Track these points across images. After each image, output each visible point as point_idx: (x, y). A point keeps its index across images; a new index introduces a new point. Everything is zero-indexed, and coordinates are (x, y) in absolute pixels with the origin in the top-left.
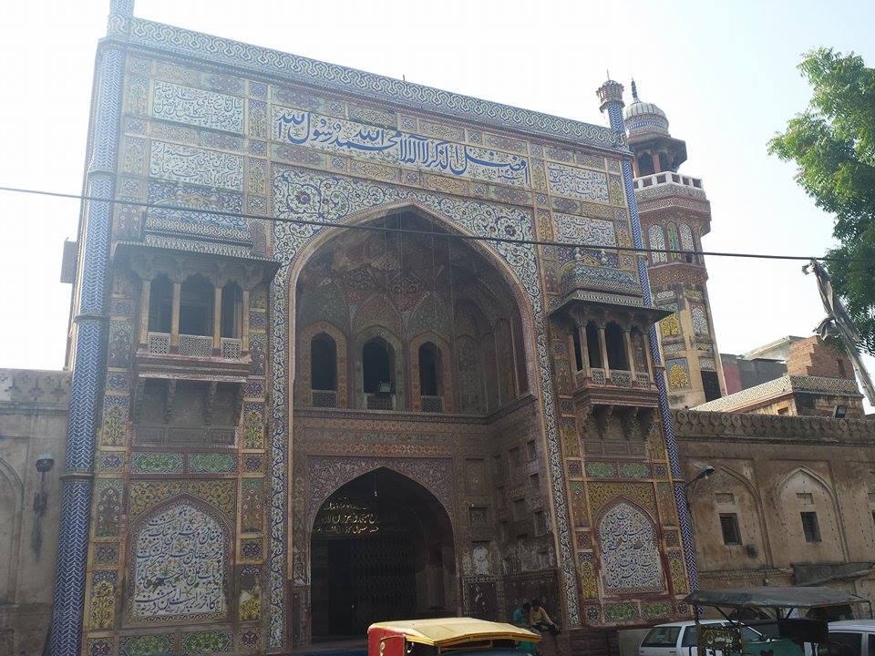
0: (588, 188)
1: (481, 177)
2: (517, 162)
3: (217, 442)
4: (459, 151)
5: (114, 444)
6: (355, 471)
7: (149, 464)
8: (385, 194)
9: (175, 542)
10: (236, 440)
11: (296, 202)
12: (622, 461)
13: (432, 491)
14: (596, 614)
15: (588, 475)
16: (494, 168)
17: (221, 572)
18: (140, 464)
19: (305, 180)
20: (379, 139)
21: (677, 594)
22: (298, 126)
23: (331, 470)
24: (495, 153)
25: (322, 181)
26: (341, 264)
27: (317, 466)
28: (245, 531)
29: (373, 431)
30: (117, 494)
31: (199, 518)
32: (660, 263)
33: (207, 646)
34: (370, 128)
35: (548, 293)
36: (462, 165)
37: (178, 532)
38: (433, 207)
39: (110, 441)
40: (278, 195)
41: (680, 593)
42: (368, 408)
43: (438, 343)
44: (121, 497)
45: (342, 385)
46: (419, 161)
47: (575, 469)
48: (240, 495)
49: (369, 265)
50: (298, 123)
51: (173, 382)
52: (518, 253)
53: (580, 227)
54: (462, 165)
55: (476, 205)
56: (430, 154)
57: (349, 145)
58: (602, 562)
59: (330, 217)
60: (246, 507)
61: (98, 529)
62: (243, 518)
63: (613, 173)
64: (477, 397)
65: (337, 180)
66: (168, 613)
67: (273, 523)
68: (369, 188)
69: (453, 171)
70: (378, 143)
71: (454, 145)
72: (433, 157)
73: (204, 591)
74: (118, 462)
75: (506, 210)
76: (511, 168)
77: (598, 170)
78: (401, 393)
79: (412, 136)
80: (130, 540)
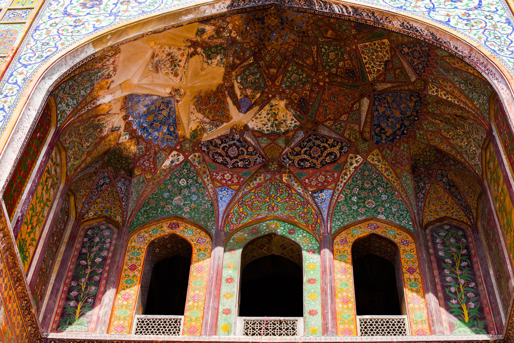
26: (193, 126)
43: (391, 234)
49: (246, 127)
52: (472, 17)
59: (127, 14)
64: (481, 310)
78: (312, 313)
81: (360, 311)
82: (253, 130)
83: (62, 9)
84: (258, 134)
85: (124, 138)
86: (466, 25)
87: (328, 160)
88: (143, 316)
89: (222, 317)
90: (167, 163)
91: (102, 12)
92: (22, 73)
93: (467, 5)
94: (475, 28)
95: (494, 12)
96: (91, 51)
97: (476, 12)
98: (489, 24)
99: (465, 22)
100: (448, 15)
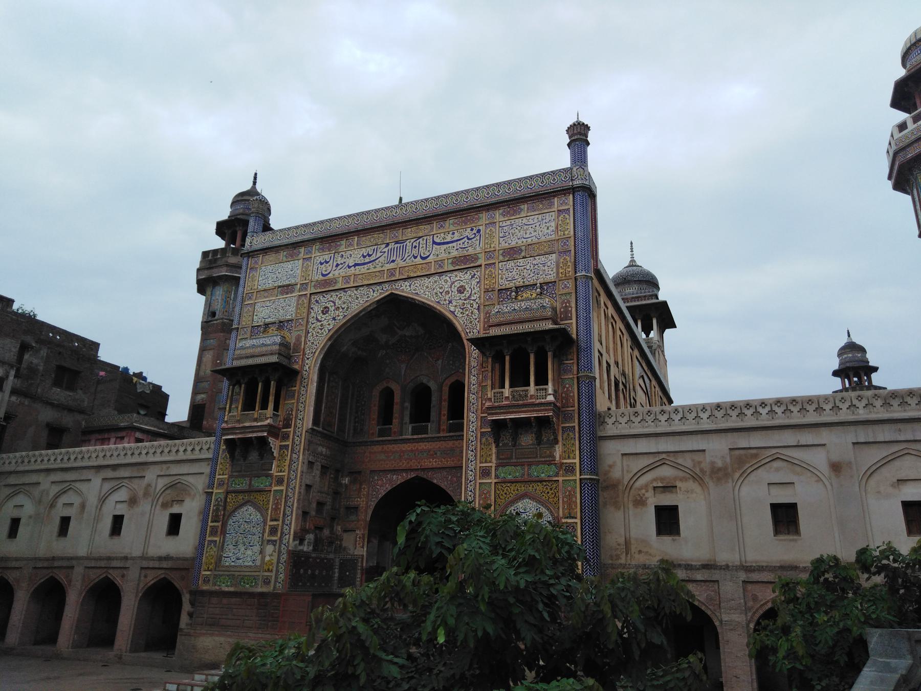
1: (443, 256)
2: (475, 231)
3: (264, 470)
4: (428, 241)
5: (223, 475)
6: (398, 479)
7: (235, 484)
8: (374, 291)
10: (273, 467)
12: (530, 464)
13: (449, 492)
15: (497, 477)
16: (454, 244)
18: (232, 484)
22: (327, 265)
23: (384, 479)
27: (376, 478)
28: (272, 520)
29: (412, 451)
30: (221, 500)
33: (248, 584)
34: (368, 249)
35: (485, 332)
38: (405, 289)
39: (221, 473)
45: (395, 421)
47: (485, 473)
48: (271, 500)
49: (405, 335)
50: (327, 262)
51: (237, 440)
54: (429, 251)
55: (436, 278)
56: (407, 251)
57: (356, 265)
59: (339, 318)
60: (274, 507)
61: (212, 518)
62: (271, 512)
63: (560, 208)
65: (346, 292)
69: (423, 258)
70: (372, 258)
71: (425, 238)
75: (460, 274)
76: (469, 239)
77: (546, 211)
78: (433, 422)
79: (397, 243)
80: (224, 525)
81: (449, 419)
86: (461, 313)
87: (439, 345)
92: (307, 364)
93: (465, 296)
94: (464, 315)
95: (474, 300)
96: (329, 343)
99: (462, 311)
100: (456, 306)
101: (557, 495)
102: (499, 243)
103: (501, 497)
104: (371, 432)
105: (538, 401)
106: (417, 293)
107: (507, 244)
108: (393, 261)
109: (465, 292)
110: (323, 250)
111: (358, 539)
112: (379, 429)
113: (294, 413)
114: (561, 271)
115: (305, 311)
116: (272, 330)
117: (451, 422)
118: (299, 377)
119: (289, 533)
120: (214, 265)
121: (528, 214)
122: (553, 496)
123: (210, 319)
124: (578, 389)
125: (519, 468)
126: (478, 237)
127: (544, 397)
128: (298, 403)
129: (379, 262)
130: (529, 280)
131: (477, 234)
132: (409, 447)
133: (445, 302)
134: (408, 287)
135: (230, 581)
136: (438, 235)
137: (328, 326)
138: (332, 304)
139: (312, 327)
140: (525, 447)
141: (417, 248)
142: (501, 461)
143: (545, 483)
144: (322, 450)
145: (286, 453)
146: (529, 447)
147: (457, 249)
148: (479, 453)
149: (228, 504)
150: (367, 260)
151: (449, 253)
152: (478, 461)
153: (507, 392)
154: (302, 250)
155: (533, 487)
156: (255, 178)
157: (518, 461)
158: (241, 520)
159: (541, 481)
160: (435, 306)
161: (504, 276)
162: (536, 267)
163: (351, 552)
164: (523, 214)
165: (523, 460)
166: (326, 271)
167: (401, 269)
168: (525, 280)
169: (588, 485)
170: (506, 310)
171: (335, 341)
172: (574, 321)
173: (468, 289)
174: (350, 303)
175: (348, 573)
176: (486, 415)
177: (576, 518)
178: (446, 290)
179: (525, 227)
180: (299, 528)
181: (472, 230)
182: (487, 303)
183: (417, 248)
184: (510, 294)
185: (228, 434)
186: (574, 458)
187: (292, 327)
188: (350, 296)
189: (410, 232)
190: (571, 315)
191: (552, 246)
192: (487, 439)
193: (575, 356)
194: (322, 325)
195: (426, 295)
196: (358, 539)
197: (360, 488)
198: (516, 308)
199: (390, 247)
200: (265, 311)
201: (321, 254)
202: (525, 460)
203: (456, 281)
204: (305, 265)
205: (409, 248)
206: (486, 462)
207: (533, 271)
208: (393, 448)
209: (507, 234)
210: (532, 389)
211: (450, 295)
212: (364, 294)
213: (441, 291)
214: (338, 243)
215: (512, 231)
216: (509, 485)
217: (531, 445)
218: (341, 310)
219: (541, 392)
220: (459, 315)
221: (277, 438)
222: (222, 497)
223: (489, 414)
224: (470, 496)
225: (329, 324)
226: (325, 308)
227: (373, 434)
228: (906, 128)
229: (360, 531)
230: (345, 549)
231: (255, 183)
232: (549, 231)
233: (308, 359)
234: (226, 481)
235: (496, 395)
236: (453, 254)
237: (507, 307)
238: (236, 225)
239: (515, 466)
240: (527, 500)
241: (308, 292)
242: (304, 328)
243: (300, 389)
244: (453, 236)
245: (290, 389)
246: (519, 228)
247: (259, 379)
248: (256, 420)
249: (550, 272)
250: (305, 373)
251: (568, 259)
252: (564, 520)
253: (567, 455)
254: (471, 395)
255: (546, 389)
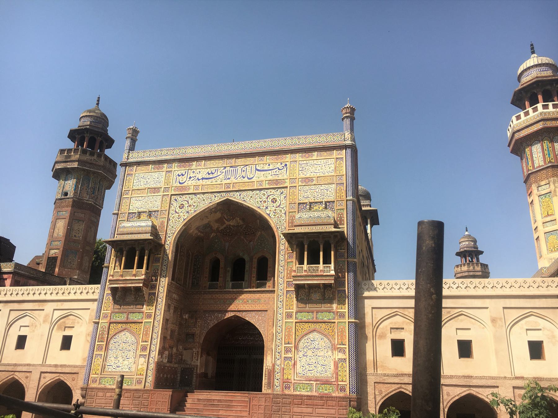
0: (322, 169)
1: (262, 178)
4: (252, 168)
7: (116, 317)
8: (215, 197)
9: (121, 345)
11: (179, 209)
13: (256, 326)
14: (289, 388)
15: (296, 318)
16: (270, 172)
17: (134, 357)
18: (113, 317)
19: (183, 199)
20: (216, 173)
21: (340, 381)
22: (183, 177)
24: (271, 164)
25: (190, 197)
26: (216, 227)
27: (207, 315)
30: (106, 328)
31: (130, 336)
32: (539, 166)
34: (212, 169)
36: (253, 174)
37: (122, 341)
38: (236, 198)
39: (106, 309)
40: (172, 208)
41: (342, 381)
42: (232, 289)
44: (107, 328)
46: (232, 178)
47: (289, 316)
50: (183, 175)
53: (314, 191)
56: (238, 173)
57: (203, 179)
58: (298, 362)
59: (191, 212)
66: (115, 370)
67: (153, 339)
68: (210, 195)
70: (215, 175)
71: (251, 166)
72: (239, 174)
73: (128, 363)
74: (107, 317)
75: (273, 191)
76: (279, 169)
78: (246, 281)
79: (231, 167)
80: (107, 344)
82: (232, 226)
83: (174, 210)
84: (234, 226)
85: (199, 234)
88: (210, 283)
89: (227, 282)
90: (212, 236)
91: (185, 211)
92: (169, 240)
93: (277, 205)
94: (276, 217)
95: (283, 208)
96: (184, 228)
97: (278, 208)
98: (280, 215)
100: (270, 211)
101: (334, 331)
102: (299, 174)
103: (299, 331)
104: (204, 285)
105: (325, 274)
106: (245, 200)
107: (304, 175)
108: (229, 179)
109: (277, 203)
110: (180, 166)
111: (194, 355)
112: (209, 284)
113: (159, 272)
114: (338, 195)
115: (168, 205)
116: (144, 216)
117: (258, 281)
118: (163, 248)
119: (156, 350)
120: (69, 160)
121: (318, 158)
122: (332, 331)
123: (63, 197)
124: (348, 267)
125: (310, 313)
126: (285, 169)
127: (329, 271)
128: (162, 265)
129: (219, 178)
130: (318, 198)
131: (285, 167)
132: (230, 296)
133: (263, 208)
134: (239, 196)
135: (112, 381)
136: (259, 165)
137: (183, 217)
138: (186, 203)
139: (172, 216)
140: (314, 301)
141: (245, 172)
142: (299, 309)
143: (326, 324)
144: (175, 296)
145: (154, 297)
146: (317, 301)
147: (272, 175)
148: (285, 303)
149: (110, 330)
150: (211, 176)
151: (266, 177)
152: (285, 308)
153: (305, 266)
154: (165, 165)
155: (319, 325)
156: (98, 101)
157: (310, 309)
158: (120, 341)
159: (324, 322)
160: (257, 209)
161: (302, 195)
162: (322, 191)
163: (189, 363)
164: (314, 158)
165: (313, 309)
166: (182, 181)
167: (234, 184)
168: (315, 198)
169: (353, 325)
170: (305, 217)
171: (187, 227)
172: (345, 226)
173: (278, 200)
174: (199, 203)
175: (187, 377)
176: (292, 280)
177: (345, 345)
178: (264, 200)
179: (316, 166)
180: (161, 347)
181: (281, 164)
182: (291, 211)
183: (245, 172)
184: (306, 206)
185: (114, 284)
186: (345, 309)
187: (158, 215)
188: (199, 198)
189: (240, 161)
190: (344, 222)
191: (332, 179)
192: (290, 295)
193: (346, 247)
194: (179, 216)
195: (250, 202)
196: (194, 355)
197: (196, 322)
198: (312, 216)
199: (227, 169)
200: (137, 205)
201: (179, 169)
202: (315, 309)
203: (270, 195)
204: (167, 175)
205: (239, 171)
206: (290, 309)
207: (320, 193)
208: (219, 296)
209: (304, 169)
210: (321, 266)
211: (267, 203)
212: (209, 198)
213: (261, 200)
214: (191, 163)
215: (307, 167)
216: (304, 324)
217: (318, 300)
218: (193, 207)
219: (327, 268)
220: (272, 216)
221: (147, 288)
222: (107, 325)
223: (294, 280)
224: (279, 330)
225: (184, 216)
226: (182, 204)
227: (205, 287)
228: (520, 119)
229: (196, 349)
230: (184, 361)
231: (98, 104)
232: (330, 170)
233: (169, 237)
234: (109, 315)
235: (298, 268)
236: (269, 178)
237: (305, 215)
238: (85, 132)
239: (308, 312)
240: (316, 333)
241: (170, 193)
242: (167, 217)
243: (164, 256)
244: (269, 167)
245: (156, 256)
246: (311, 166)
247: (137, 249)
248: (135, 275)
249: (331, 195)
250: (167, 246)
251: (342, 188)
252: (339, 346)
253: (340, 308)
254: (280, 267)
255: (330, 267)
